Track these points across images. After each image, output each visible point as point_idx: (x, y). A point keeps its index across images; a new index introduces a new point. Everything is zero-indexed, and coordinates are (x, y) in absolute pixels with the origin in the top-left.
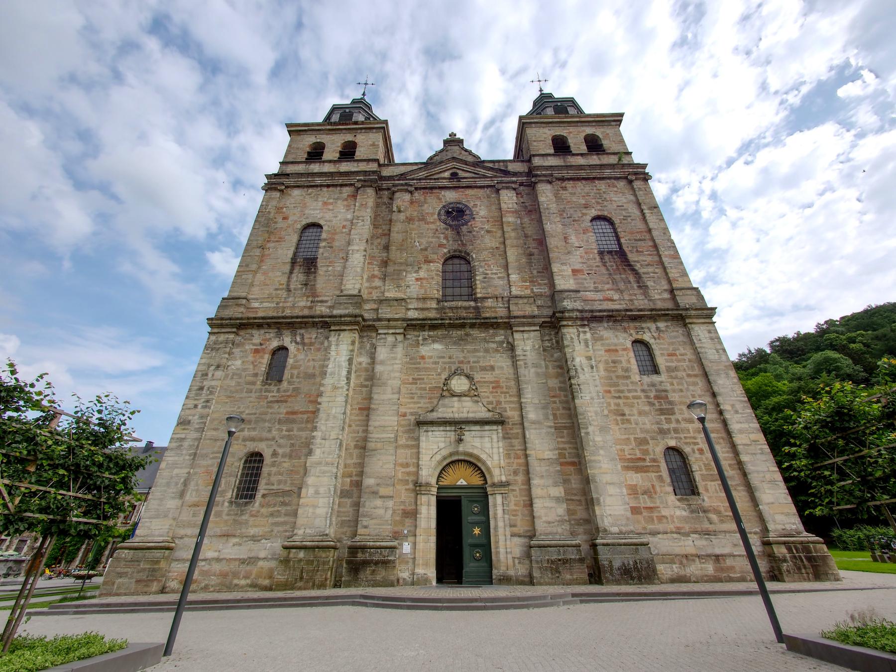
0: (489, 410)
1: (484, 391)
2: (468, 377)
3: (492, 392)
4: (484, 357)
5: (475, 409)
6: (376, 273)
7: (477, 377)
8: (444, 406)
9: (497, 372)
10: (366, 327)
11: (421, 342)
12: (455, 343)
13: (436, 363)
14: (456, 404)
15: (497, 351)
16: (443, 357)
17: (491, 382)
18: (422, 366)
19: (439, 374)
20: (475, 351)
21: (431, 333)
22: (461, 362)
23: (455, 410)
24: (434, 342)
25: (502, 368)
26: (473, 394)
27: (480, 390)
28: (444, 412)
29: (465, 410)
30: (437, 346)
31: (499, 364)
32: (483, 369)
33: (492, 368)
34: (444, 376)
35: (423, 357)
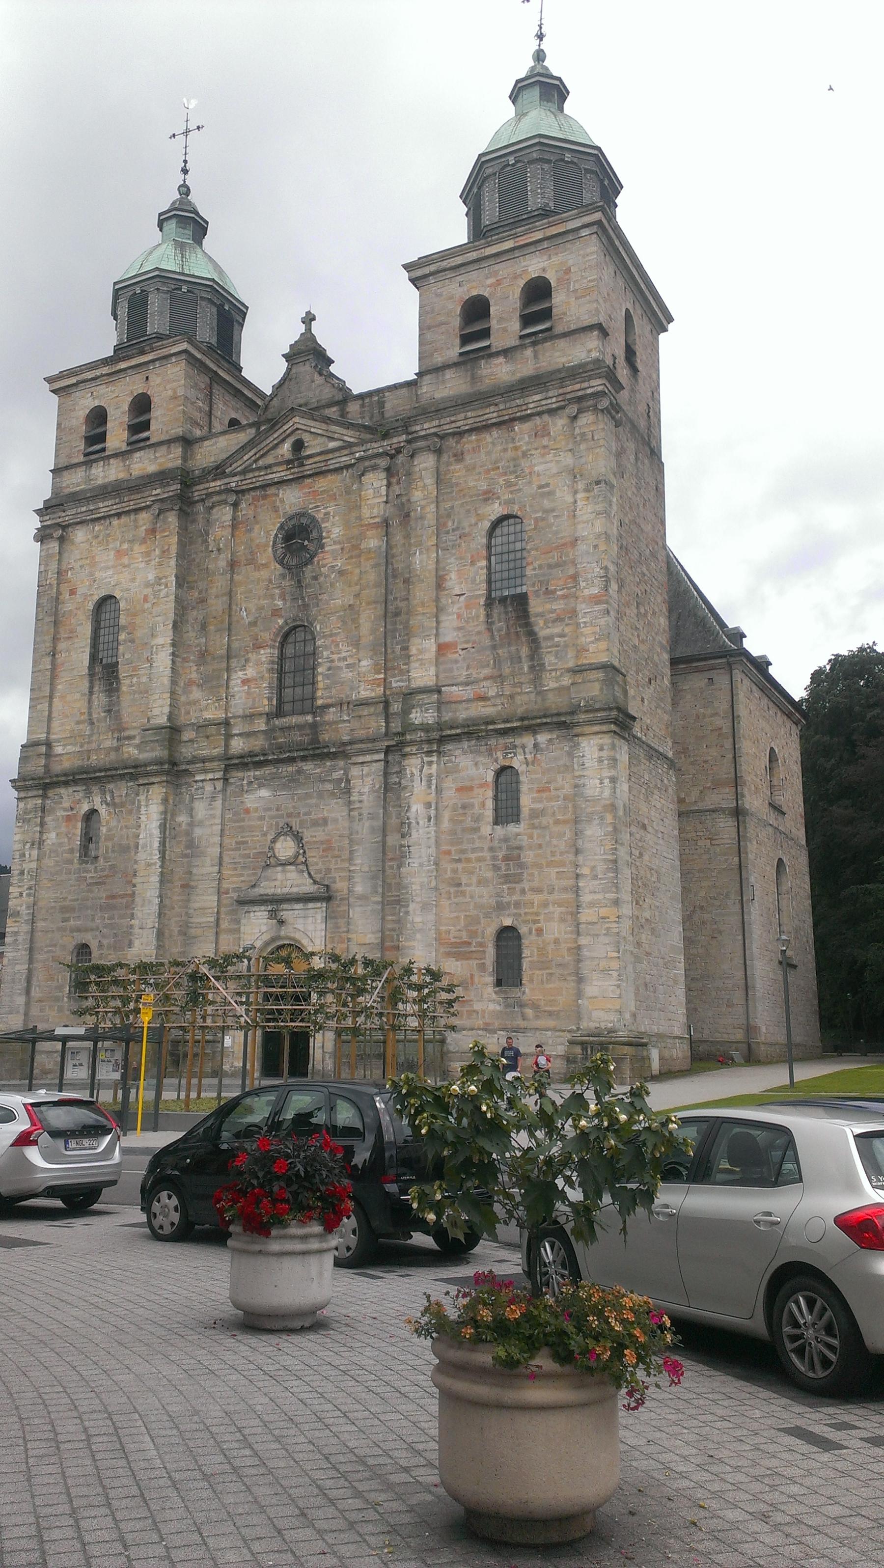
0: (315, 882)
1: (314, 857)
2: (298, 838)
3: (321, 857)
4: (317, 806)
5: (300, 882)
6: (194, 676)
7: (307, 835)
8: (267, 879)
9: (330, 827)
10: (175, 771)
11: (245, 788)
12: (285, 786)
13: (262, 818)
14: (279, 876)
15: (332, 794)
16: (270, 809)
17: (322, 842)
18: (246, 823)
19: (265, 835)
20: (308, 796)
21: (257, 773)
22: (290, 815)
23: (277, 883)
24: (261, 786)
25: (336, 820)
26: (298, 861)
27: (308, 854)
28: (267, 888)
29: (289, 883)
30: (264, 793)
31: (333, 815)
32: (315, 824)
33: (325, 821)
34: (270, 837)
35: (247, 811)
